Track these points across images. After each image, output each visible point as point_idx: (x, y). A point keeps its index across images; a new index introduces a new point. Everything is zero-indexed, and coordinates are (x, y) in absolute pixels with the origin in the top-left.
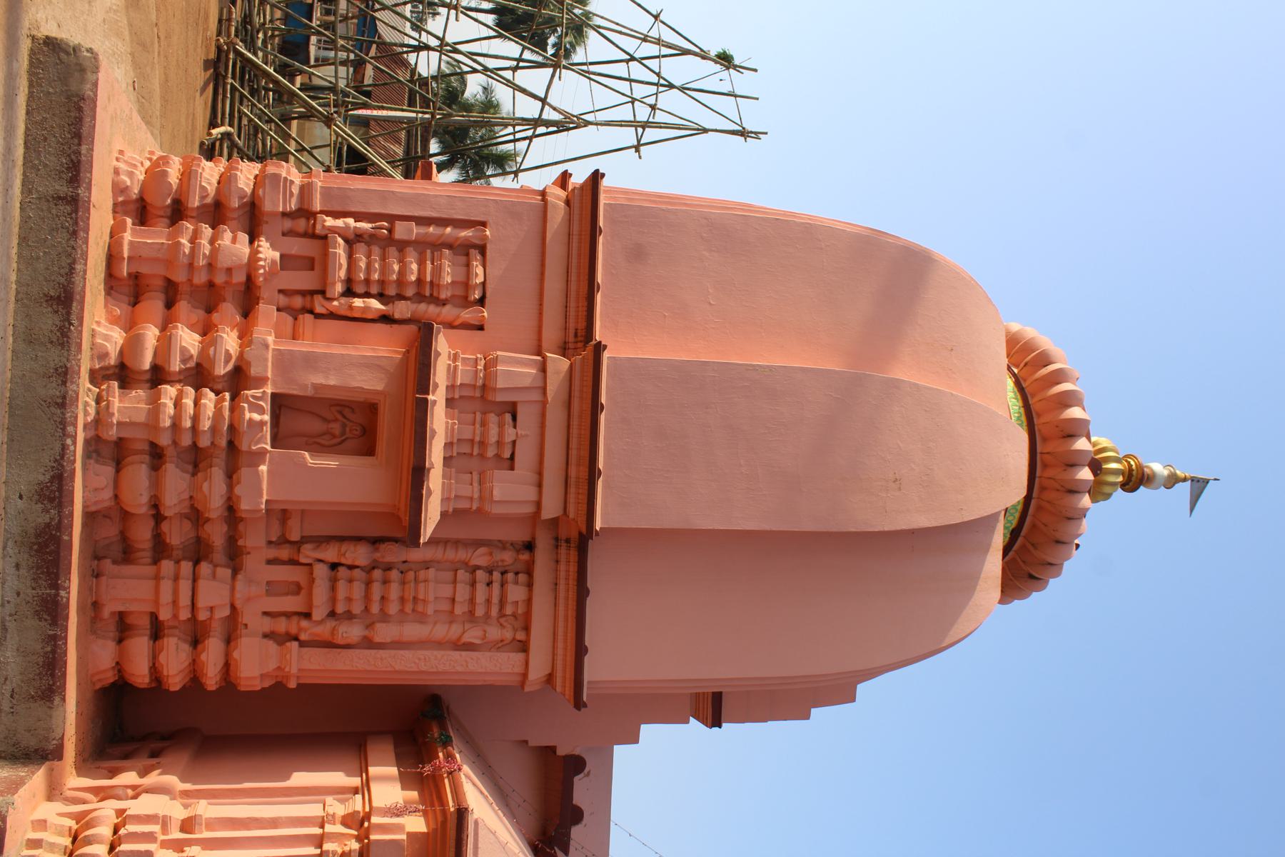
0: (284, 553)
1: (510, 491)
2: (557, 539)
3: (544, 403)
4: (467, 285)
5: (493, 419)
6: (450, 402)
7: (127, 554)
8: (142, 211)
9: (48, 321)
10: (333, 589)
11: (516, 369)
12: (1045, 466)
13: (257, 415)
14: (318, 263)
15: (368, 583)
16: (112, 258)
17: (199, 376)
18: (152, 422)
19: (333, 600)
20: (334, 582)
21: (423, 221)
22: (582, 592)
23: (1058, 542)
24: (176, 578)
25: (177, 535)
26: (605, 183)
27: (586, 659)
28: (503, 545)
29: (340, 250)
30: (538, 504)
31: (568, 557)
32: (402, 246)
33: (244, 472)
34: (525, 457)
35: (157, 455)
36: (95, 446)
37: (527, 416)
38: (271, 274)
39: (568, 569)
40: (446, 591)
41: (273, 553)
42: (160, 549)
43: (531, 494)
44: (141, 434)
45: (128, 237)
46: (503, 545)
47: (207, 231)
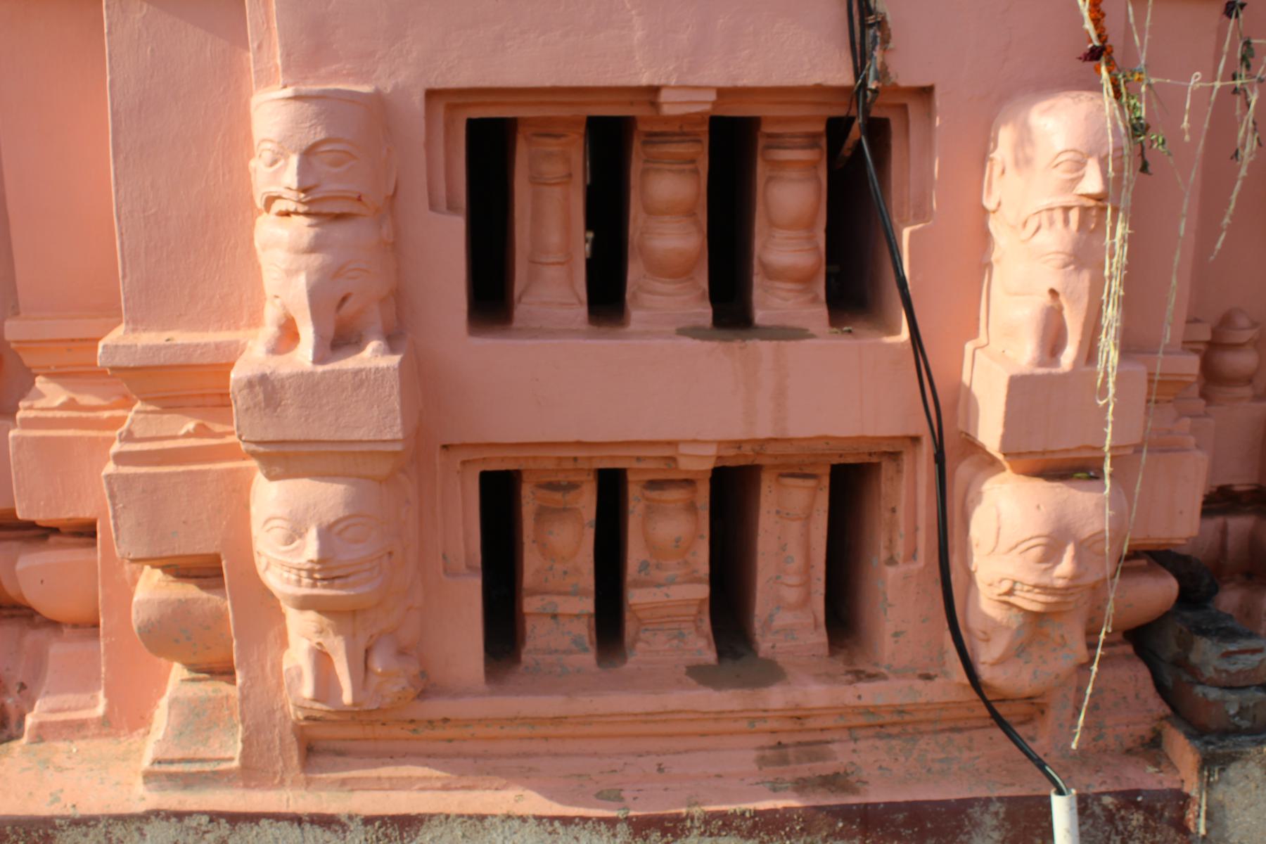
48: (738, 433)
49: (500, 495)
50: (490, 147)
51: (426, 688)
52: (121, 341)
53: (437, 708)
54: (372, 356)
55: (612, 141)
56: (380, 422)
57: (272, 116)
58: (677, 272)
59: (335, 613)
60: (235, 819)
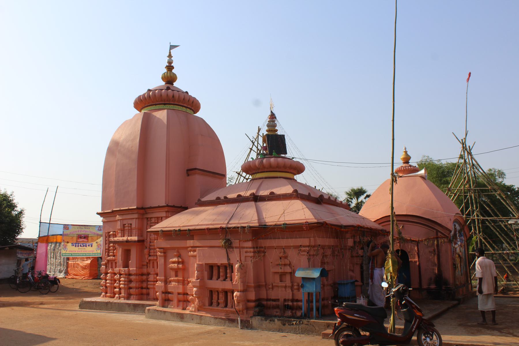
2: (146, 213)
4: (113, 235)
6: (124, 236)
7: (148, 294)
8: (106, 293)
10: (152, 256)
11: (118, 226)
13: (123, 270)
16: (111, 297)
18: (124, 288)
20: (152, 256)
21: (106, 244)
22: (151, 208)
23: (161, 95)
25: (144, 285)
26: (100, 211)
27: (161, 205)
28: (147, 224)
30: (136, 218)
31: (149, 211)
32: (109, 247)
33: (131, 272)
34: (130, 222)
35: (130, 288)
36: (128, 298)
37: (125, 222)
43: (135, 220)
45: (108, 295)
46: (147, 224)
47: (108, 281)
50: (211, 267)
55: (219, 267)
56: (198, 285)
57: (196, 265)
58: (223, 276)
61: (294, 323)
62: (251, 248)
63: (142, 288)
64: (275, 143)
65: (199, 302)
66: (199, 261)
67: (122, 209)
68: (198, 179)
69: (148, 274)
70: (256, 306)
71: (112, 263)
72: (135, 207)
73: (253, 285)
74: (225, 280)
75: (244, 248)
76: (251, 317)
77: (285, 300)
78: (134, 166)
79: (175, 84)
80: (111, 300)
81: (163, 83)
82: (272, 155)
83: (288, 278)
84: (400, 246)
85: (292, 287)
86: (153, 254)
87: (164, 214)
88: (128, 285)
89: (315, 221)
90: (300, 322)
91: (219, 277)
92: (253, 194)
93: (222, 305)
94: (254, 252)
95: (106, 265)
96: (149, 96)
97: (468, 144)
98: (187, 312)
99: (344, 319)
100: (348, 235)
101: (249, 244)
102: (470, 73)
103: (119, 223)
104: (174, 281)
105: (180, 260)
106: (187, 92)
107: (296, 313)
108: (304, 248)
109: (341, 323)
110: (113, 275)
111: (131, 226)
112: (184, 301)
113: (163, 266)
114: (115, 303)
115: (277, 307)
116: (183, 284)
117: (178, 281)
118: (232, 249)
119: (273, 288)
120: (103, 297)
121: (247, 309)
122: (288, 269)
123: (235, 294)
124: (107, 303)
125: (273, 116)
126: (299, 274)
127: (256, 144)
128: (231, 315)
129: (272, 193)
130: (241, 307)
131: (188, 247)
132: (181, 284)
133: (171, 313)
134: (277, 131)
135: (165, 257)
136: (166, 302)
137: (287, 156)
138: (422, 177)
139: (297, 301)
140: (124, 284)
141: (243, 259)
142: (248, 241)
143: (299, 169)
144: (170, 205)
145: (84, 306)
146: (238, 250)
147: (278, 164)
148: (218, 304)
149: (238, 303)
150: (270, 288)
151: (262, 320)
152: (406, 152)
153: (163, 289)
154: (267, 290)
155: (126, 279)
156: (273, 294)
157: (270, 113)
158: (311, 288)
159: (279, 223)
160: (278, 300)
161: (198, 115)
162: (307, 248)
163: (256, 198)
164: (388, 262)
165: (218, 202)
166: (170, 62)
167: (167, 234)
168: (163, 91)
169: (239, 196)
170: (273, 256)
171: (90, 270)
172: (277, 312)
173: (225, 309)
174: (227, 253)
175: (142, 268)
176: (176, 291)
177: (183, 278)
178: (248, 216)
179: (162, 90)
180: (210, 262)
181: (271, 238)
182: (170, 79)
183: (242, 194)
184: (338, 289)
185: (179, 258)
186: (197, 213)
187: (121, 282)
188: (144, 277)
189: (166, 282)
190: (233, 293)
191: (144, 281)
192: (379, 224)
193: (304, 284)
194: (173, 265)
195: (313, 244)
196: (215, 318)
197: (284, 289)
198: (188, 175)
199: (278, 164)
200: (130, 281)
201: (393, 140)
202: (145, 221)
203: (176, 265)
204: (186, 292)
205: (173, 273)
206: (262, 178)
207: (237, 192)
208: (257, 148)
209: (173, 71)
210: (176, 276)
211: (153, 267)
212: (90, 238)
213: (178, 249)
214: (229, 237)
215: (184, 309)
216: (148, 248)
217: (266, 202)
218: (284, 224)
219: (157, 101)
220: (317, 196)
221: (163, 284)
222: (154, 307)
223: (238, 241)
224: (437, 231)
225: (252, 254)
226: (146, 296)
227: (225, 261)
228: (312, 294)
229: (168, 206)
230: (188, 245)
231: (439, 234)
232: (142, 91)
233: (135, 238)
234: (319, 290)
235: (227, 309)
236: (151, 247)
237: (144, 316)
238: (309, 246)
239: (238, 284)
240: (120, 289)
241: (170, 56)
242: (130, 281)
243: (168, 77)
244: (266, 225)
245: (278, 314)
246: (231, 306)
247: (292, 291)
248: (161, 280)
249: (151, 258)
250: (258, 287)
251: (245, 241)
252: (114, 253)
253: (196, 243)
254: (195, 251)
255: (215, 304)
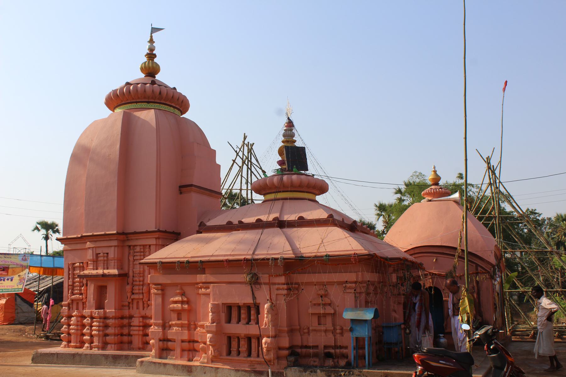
0: (131, 305)
1: (112, 253)
2: (128, 240)
3: (96, 247)
4: (80, 267)
5: (100, 259)
6: (97, 269)
7: (130, 343)
9: (77, 358)
10: (137, 293)
11: (90, 255)
12: (128, 100)
13: (96, 313)
14: (76, 301)
15: (137, 285)
16: (76, 347)
17: (91, 326)
18: (98, 335)
19: (139, 293)
20: (137, 293)
21: (69, 279)
23: (145, 91)
24: (134, 330)
25: (125, 331)
27: (149, 230)
28: (129, 253)
29: (73, 297)
30: (115, 246)
32: (74, 283)
33: (108, 315)
34: (106, 250)
35: (106, 335)
36: (103, 348)
38: (79, 312)
39: (132, 237)
40: (138, 266)
41: (131, 308)
42: (129, 335)
43: (113, 248)
44: (101, 339)
45: (72, 344)
46: (129, 253)
47: (71, 327)
48: (245, 333)
49: (229, 338)
50: (229, 308)
51: (221, 355)
52: (202, 323)
53: (221, 357)
54: (215, 324)
55: (239, 307)
56: (214, 329)
57: (210, 305)
59: (213, 346)
60: (205, 366)
61: (342, 374)
62: (284, 284)
63: (122, 335)
64: (294, 156)
65: (214, 351)
66: (214, 300)
67: (95, 234)
68: (194, 198)
69: (131, 317)
70: (291, 354)
71: (78, 303)
72: (115, 232)
73: (286, 329)
74: (248, 323)
75: (275, 284)
76: (286, 368)
77: (326, 347)
78: (113, 180)
79: (158, 77)
80: (80, 351)
81: (143, 76)
82: (292, 171)
83: (329, 320)
84: (433, 282)
85: (334, 332)
86: (137, 291)
87: (153, 242)
88: (103, 331)
89: (366, 252)
90: (349, 372)
91: (239, 321)
92: (274, 219)
93: (244, 354)
94: (289, 289)
95: (68, 305)
96: (129, 91)
97: (494, 163)
98: (197, 364)
99: (426, 367)
100: (391, 269)
101: (282, 279)
102: (506, 82)
103: (90, 252)
104: (176, 325)
105: (185, 299)
106: (175, 88)
107: (338, 362)
108: (350, 285)
109: (422, 372)
110: (79, 319)
111: (107, 256)
112: (189, 350)
113: (161, 307)
114: (86, 355)
115: (316, 355)
116: (189, 330)
117: (182, 326)
118: (259, 286)
119: (308, 333)
120: (65, 347)
121: (278, 358)
122: (330, 310)
123: (264, 341)
124: (74, 355)
125: (290, 124)
126: (348, 315)
127: (241, 154)
128: (256, 366)
129: (301, 218)
130: (272, 356)
131: (198, 283)
132: (186, 328)
133: (174, 365)
134: (295, 141)
135: (163, 296)
136: (164, 351)
137: (311, 171)
138: (456, 201)
139: (341, 347)
140: (99, 331)
141: (274, 297)
142: (280, 276)
143: (322, 188)
144: (161, 229)
145: (38, 359)
146: (268, 286)
147: (301, 182)
148: (239, 353)
149: (268, 351)
150: (304, 333)
151: (300, 371)
152: (435, 172)
153: (160, 336)
154: (301, 335)
155: (101, 324)
156: (311, 340)
157: (285, 120)
158: (364, 332)
159: (319, 254)
160: (316, 347)
161: (183, 116)
162: (354, 285)
163: (280, 224)
164: (464, 301)
165: (229, 227)
166: (151, 49)
167: (168, 267)
168: (148, 85)
169: (259, 220)
170: (309, 295)
171: (5, 312)
172: (315, 361)
173: (249, 359)
174: (252, 291)
175: (121, 309)
176: (178, 338)
177: (188, 321)
178: (277, 245)
179: (146, 84)
180: (229, 301)
181: (309, 273)
182: (151, 70)
183: (264, 218)
184: (383, 333)
185: (183, 297)
186: (208, 241)
187: (94, 328)
188: (126, 321)
189: (165, 326)
190: (259, 339)
191: (125, 326)
192: (411, 255)
193: (354, 327)
194: (175, 305)
195: (360, 279)
196: (236, 370)
197: (323, 334)
198: (181, 193)
199: (301, 182)
200: (106, 326)
201: (466, 160)
202: (127, 249)
203: (180, 305)
204: (192, 338)
205: (174, 316)
206: (286, 199)
207: (256, 216)
208: (242, 159)
209: (156, 60)
210: (179, 319)
211: (138, 308)
212: (10, 270)
213: (182, 285)
214: (255, 271)
215: (189, 360)
216: (130, 283)
217: (295, 229)
218: (326, 256)
219: (139, 98)
220: (350, 223)
221: (160, 330)
222: (148, 358)
223: (268, 275)
224: (477, 265)
225: (285, 292)
226: (127, 345)
227: (249, 300)
228: (364, 339)
229: (159, 231)
230: (198, 281)
231: (479, 269)
232: (118, 84)
233: (115, 272)
234: (370, 335)
235: (252, 359)
236: (134, 283)
237: (135, 371)
238: (355, 282)
239: (268, 328)
240: (92, 336)
241: (151, 41)
242: (106, 326)
243: (149, 68)
244: (302, 257)
245: (316, 363)
246: (256, 355)
247: (334, 336)
248: (156, 325)
249: (136, 296)
250: (291, 331)
251: (277, 276)
252: (80, 290)
253: (211, 278)
254: (208, 288)
255: (254, 352)
